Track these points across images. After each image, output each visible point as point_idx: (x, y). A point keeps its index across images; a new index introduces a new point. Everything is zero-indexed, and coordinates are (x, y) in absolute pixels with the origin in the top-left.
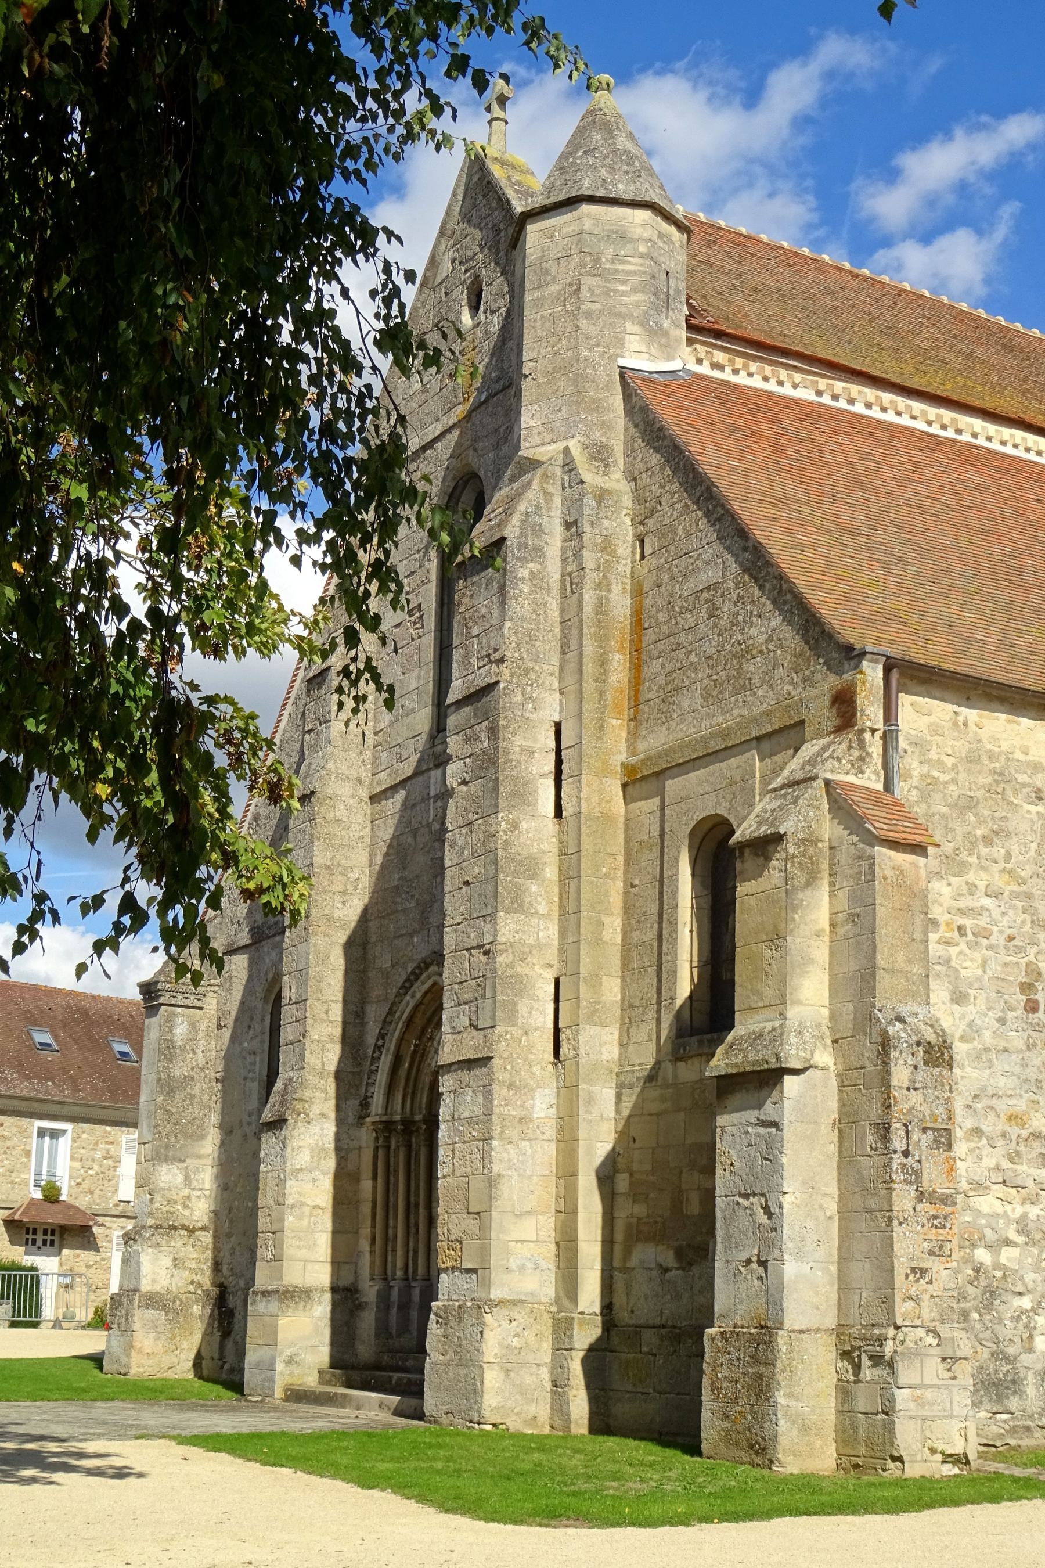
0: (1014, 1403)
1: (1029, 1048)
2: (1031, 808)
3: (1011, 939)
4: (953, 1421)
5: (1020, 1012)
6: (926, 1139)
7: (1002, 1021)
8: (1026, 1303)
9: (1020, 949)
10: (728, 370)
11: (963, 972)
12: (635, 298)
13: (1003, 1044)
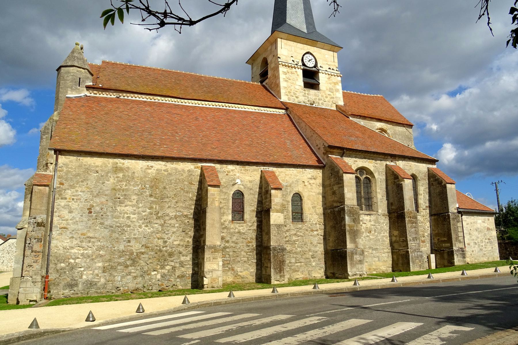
0: (75, 289)
1: (88, 220)
2: (95, 174)
3: (86, 200)
4: (33, 294)
5: (87, 214)
6: (34, 241)
7: (82, 216)
8: (82, 269)
9: (88, 202)
10: (98, 94)
11: (72, 207)
12: (70, 84)
13: (81, 220)
